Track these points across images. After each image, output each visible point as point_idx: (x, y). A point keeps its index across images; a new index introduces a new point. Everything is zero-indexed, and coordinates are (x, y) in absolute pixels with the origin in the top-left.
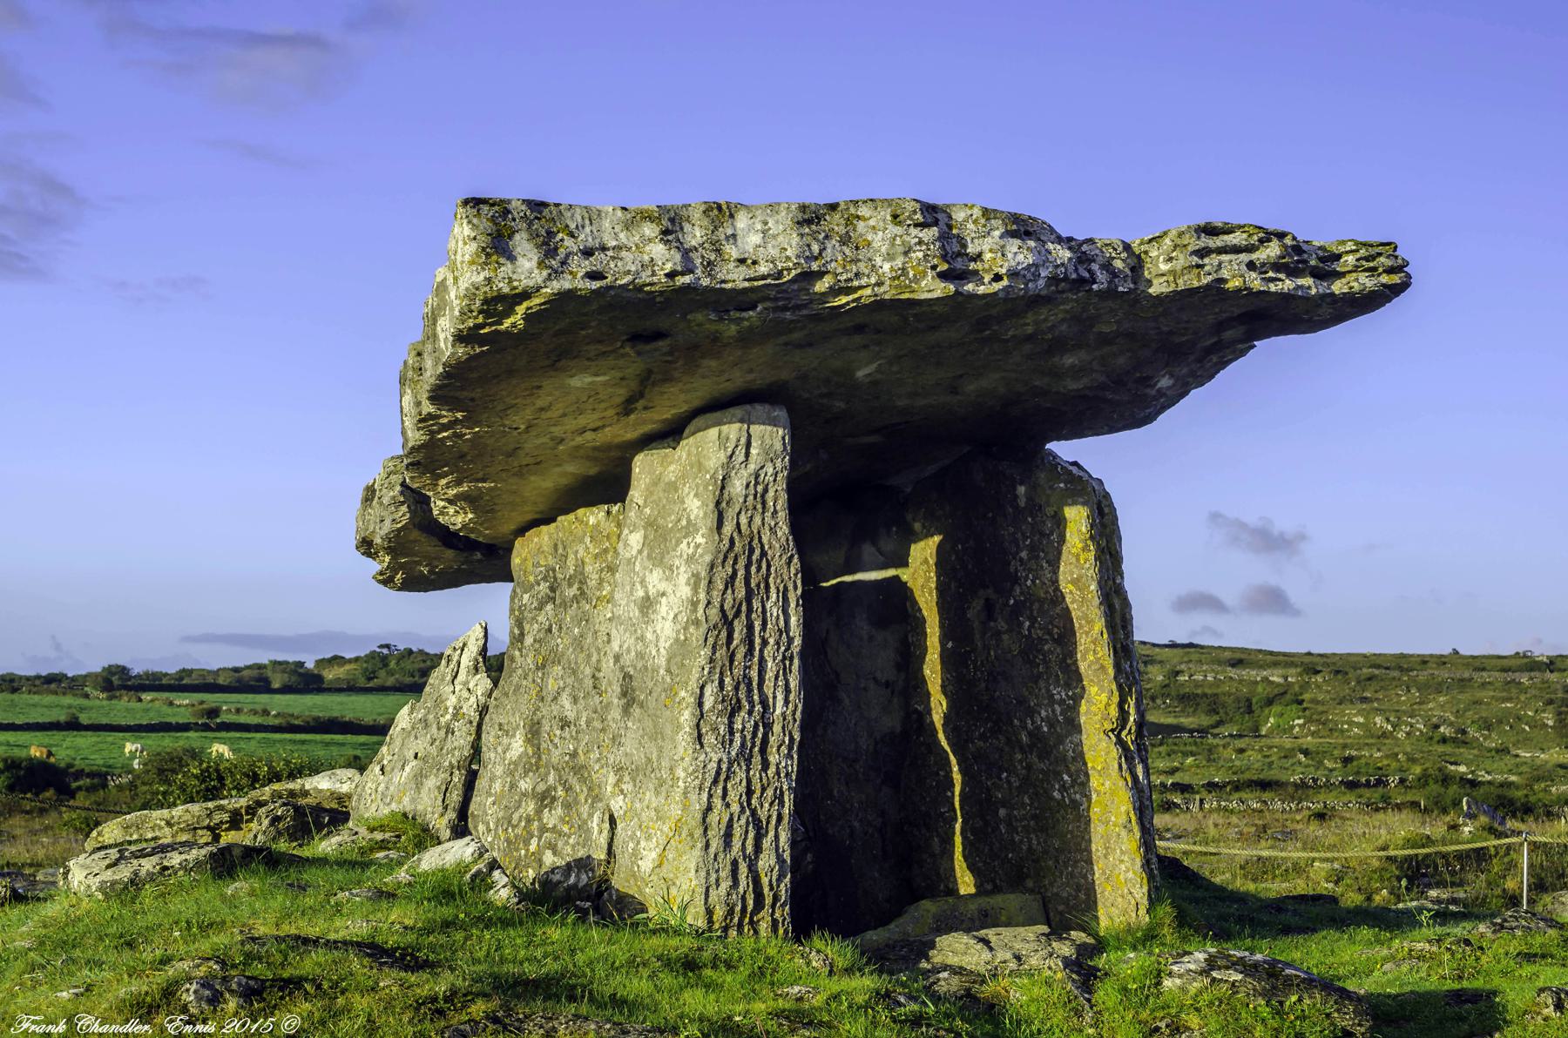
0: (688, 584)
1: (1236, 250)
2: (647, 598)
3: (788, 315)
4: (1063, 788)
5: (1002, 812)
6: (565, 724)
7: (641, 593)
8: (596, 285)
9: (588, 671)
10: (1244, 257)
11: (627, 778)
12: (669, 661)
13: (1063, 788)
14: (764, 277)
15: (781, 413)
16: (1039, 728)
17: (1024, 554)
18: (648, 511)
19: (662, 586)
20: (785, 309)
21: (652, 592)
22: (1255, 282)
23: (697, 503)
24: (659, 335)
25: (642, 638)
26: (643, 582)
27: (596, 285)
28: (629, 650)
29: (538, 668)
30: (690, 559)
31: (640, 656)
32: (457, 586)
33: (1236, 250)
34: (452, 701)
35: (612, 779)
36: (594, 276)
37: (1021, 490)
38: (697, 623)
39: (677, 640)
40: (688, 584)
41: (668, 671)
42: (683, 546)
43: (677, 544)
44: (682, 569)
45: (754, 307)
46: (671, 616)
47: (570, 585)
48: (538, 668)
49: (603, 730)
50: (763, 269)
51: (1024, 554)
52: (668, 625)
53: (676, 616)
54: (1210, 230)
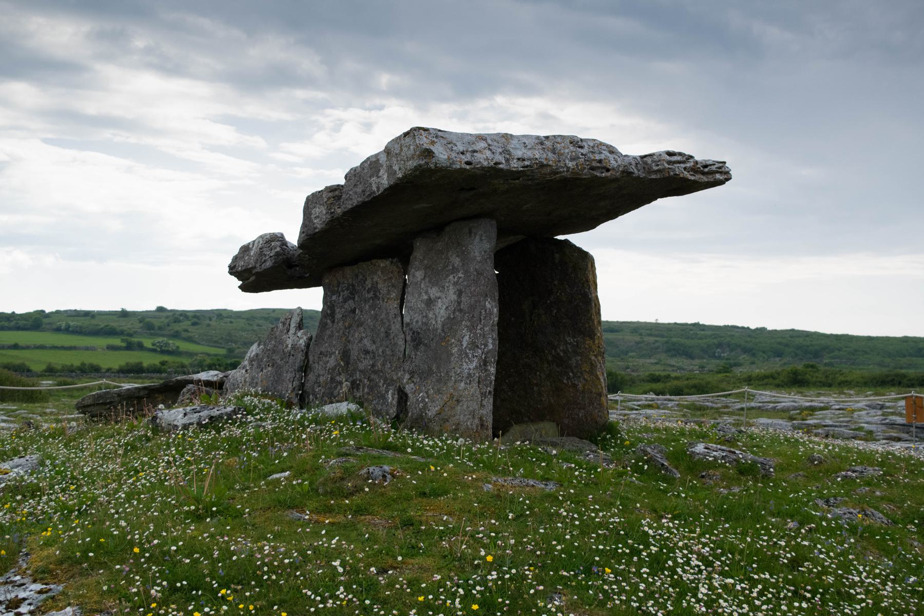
0: (455, 293)
1: (679, 162)
3: (530, 183)
4: (569, 378)
5: (535, 388)
6: (367, 352)
7: (426, 297)
8: (468, 167)
9: (382, 330)
10: (683, 165)
11: (416, 376)
12: (443, 326)
13: (569, 378)
14: (527, 166)
15: (494, 222)
16: (558, 354)
17: (556, 282)
18: (426, 262)
19: (439, 294)
20: (529, 180)
21: (432, 297)
22: (687, 175)
24: (472, 189)
25: (426, 316)
26: (426, 293)
27: (468, 167)
28: (417, 322)
29: (346, 328)
30: (455, 284)
31: (426, 324)
32: (257, 292)
33: (679, 162)
34: (289, 342)
35: (407, 376)
36: (468, 163)
37: (557, 256)
38: (461, 310)
39: (449, 318)
40: (455, 293)
41: (443, 330)
42: (451, 277)
43: (447, 276)
44: (451, 287)
45: (518, 179)
46: (444, 307)
47: (368, 292)
48: (346, 328)
50: (527, 163)
51: (556, 282)
52: (442, 311)
53: (447, 308)
54: (670, 154)
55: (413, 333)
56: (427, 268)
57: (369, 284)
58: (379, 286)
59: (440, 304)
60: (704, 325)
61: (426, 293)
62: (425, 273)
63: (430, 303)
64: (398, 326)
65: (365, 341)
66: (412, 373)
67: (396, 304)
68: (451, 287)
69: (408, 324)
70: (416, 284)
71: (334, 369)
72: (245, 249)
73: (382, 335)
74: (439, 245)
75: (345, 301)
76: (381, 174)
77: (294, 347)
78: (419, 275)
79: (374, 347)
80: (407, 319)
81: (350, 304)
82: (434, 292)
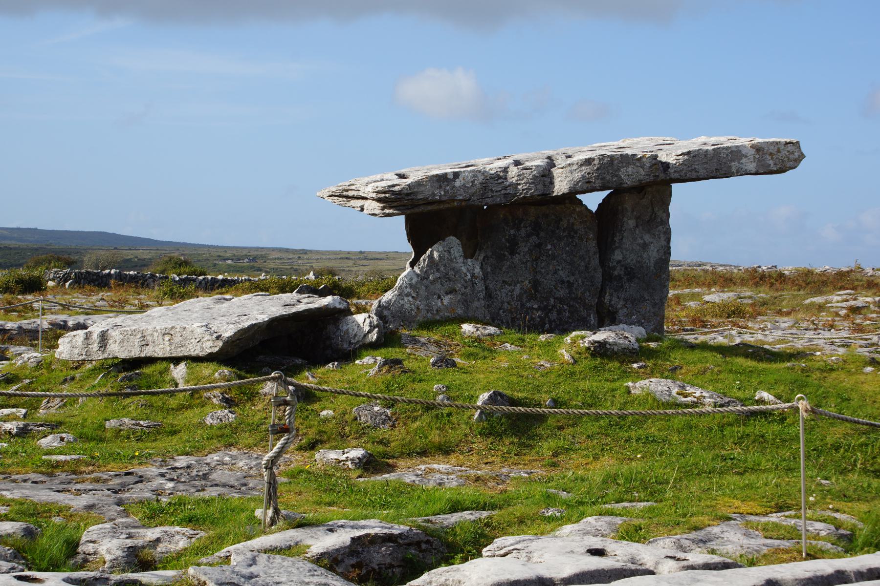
2: (645, 243)
6: (562, 282)
9: (583, 264)
19: (651, 240)
23: (665, 215)
26: (642, 238)
28: (632, 260)
31: (639, 262)
35: (622, 303)
39: (661, 259)
42: (660, 228)
43: (657, 227)
44: (662, 235)
47: (564, 231)
49: (592, 285)
52: (655, 254)
55: (626, 268)
56: (637, 218)
57: (564, 224)
58: (575, 227)
59: (652, 248)
60: (824, 273)
61: (642, 238)
62: (637, 223)
63: (645, 246)
64: (597, 261)
65: (561, 273)
66: (626, 300)
67: (592, 245)
68: (662, 235)
69: (619, 262)
70: (630, 229)
71: (520, 297)
72: (442, 179)
73: (582, 268)
74: (645, 202)
75: (529, 236)
76: (744, 160)
77: (473, 276)
78: (631, 223)
79: (572, 279)
80: (618, 256)
81: (534, 239)
82: (647, 238)
